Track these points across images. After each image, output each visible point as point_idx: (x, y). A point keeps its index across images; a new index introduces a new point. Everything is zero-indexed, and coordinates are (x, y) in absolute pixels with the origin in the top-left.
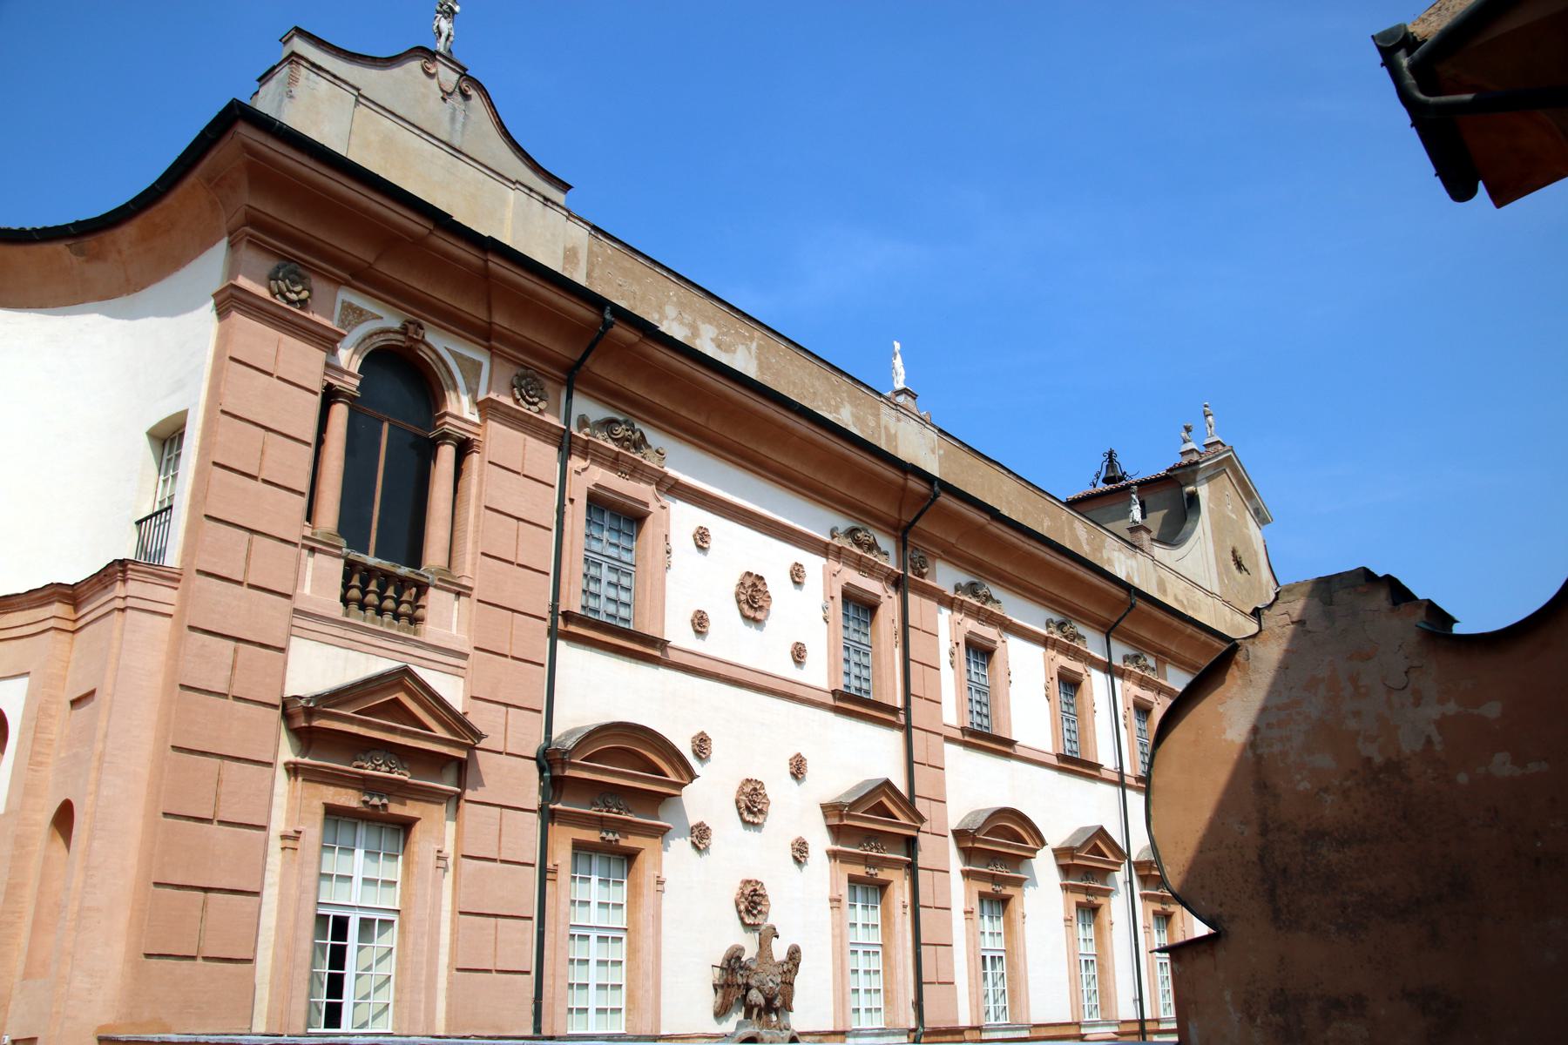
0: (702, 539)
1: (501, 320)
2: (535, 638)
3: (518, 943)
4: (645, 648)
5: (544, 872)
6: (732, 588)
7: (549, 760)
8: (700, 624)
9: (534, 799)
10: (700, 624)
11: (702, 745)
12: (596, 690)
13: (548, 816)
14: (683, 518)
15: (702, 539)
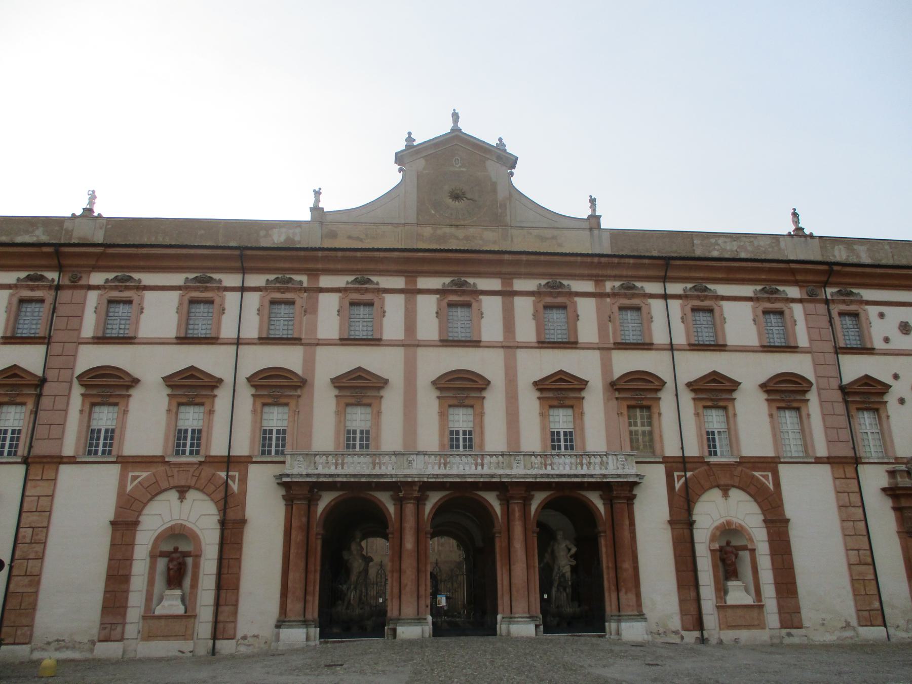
0: (882, 315)
1: (799, 278)
2: (831, 358)
3: (845, 435)
4: (869, 351)
5: (849, 417)
6: (898, 325)
7: (842, 389)
8: (887, 340)
9: (841, 400)
10: (887, 340)
11: (896, 377)
12: (853, 368)
13: (846, 402)
14: (873, 311)
15: (882, 315)
